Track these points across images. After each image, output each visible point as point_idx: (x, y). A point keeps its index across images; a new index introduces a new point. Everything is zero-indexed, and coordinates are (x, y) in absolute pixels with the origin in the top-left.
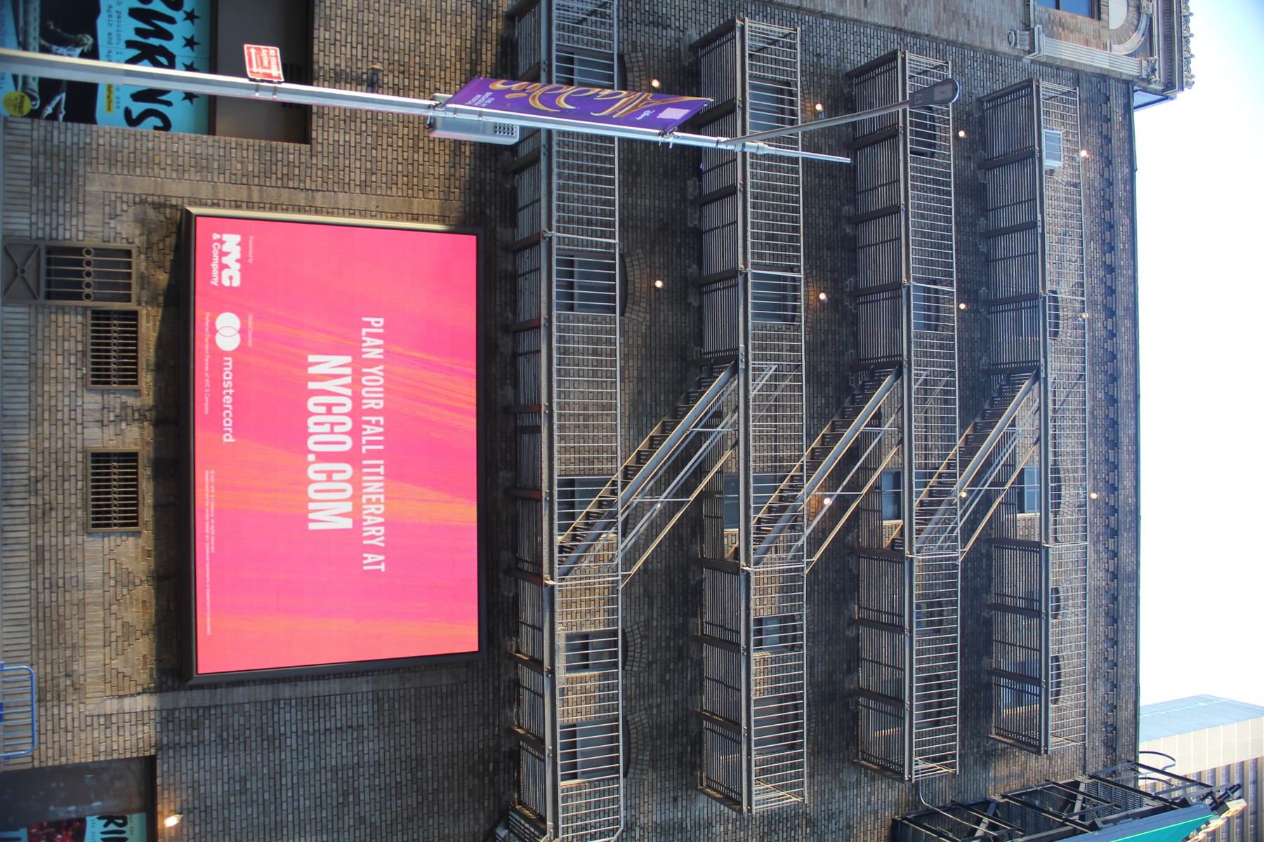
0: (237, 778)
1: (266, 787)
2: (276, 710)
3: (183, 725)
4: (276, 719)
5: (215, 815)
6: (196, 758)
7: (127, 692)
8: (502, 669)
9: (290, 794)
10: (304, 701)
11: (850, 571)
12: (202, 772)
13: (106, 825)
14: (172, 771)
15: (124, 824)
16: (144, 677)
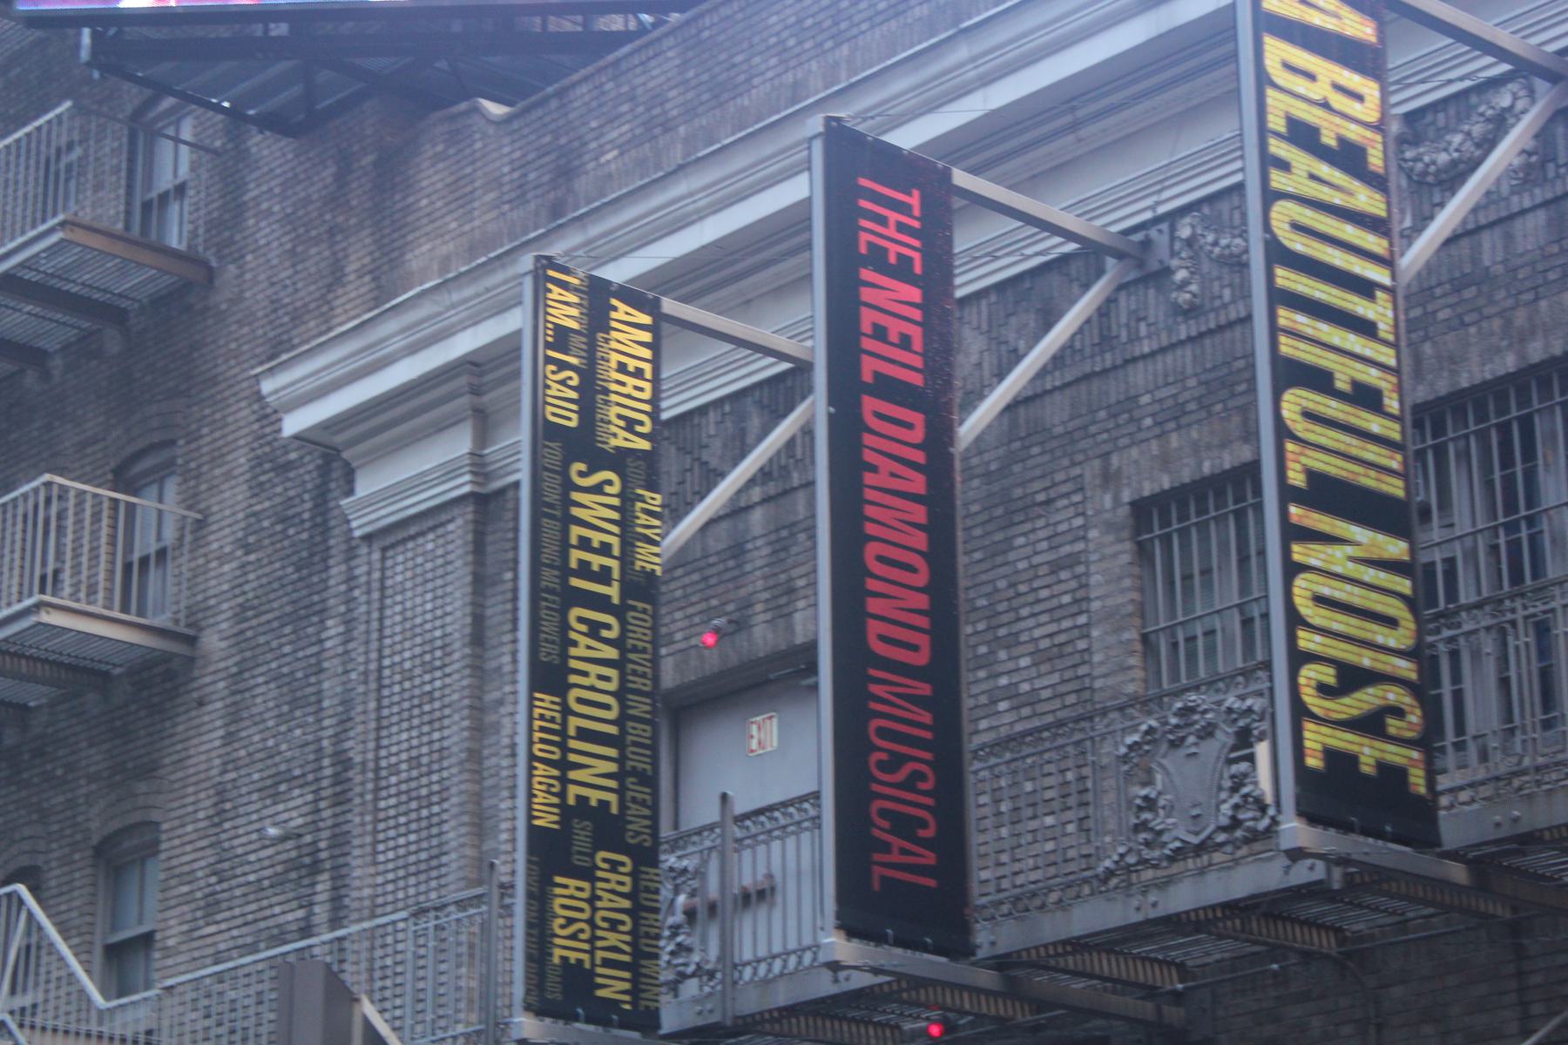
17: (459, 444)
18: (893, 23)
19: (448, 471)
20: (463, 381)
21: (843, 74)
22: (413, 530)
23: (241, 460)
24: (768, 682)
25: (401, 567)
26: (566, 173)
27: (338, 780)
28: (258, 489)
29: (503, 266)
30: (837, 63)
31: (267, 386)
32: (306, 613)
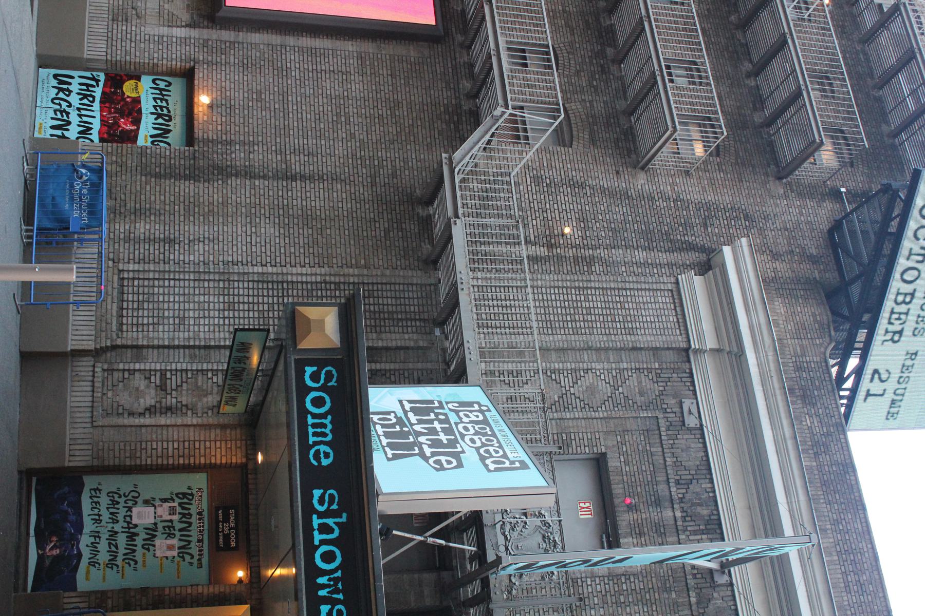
0: (254, 90)
1: (276, 100)
2: (283, 51)
3: (214, 50)
4: (284, 57)
5: (237, 111)
6: (223, 73)
7: (174, 24)
8: (457, 54)
9: (295, 108)
10: (305, 50)
11: (739, 40)
12: (228, 82)
13: (156, 119)
14: (206, 78)
15: (170, 120)
16: (185, 17)
17: (711, 343)
18: (842, 585)
19: (701, 335)
20: (735, 349)
21: (828, 559)
22: (678, 309)
23: (711, 198)
24: (606, 519)
25: (665, 300)
26: (804, 397)
27: (584, 258)
28: (699, 206)
29: (780, 388)
30: (831, 555)
31: (744, 241)
32: (649, 240)
